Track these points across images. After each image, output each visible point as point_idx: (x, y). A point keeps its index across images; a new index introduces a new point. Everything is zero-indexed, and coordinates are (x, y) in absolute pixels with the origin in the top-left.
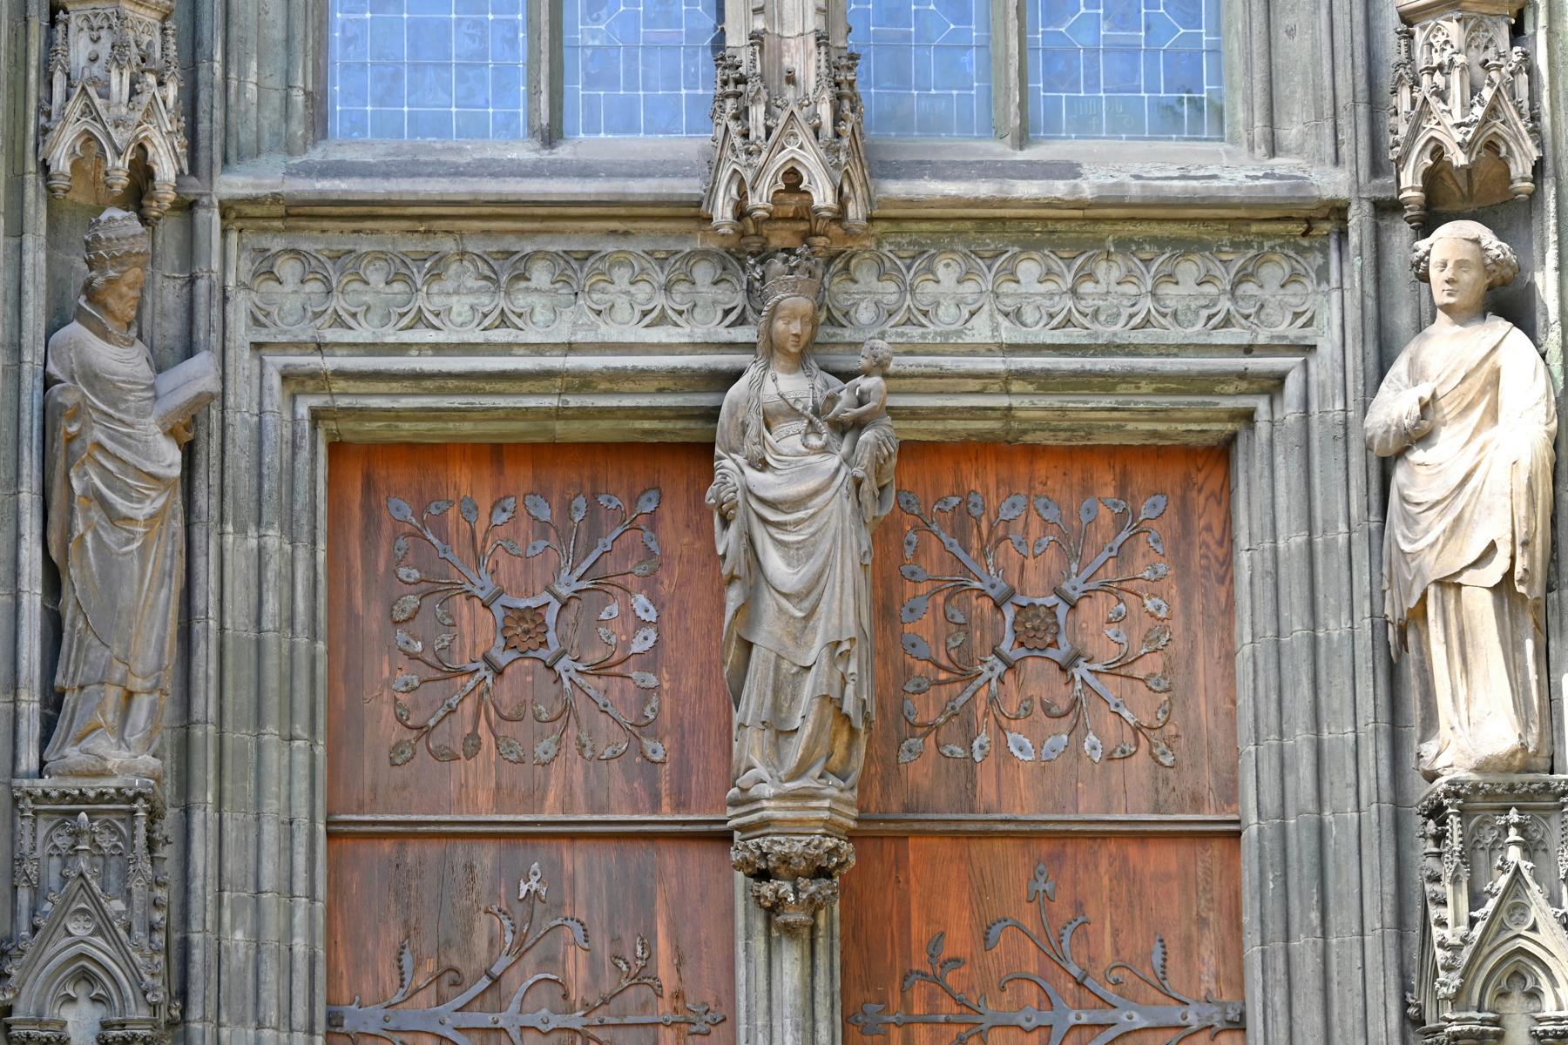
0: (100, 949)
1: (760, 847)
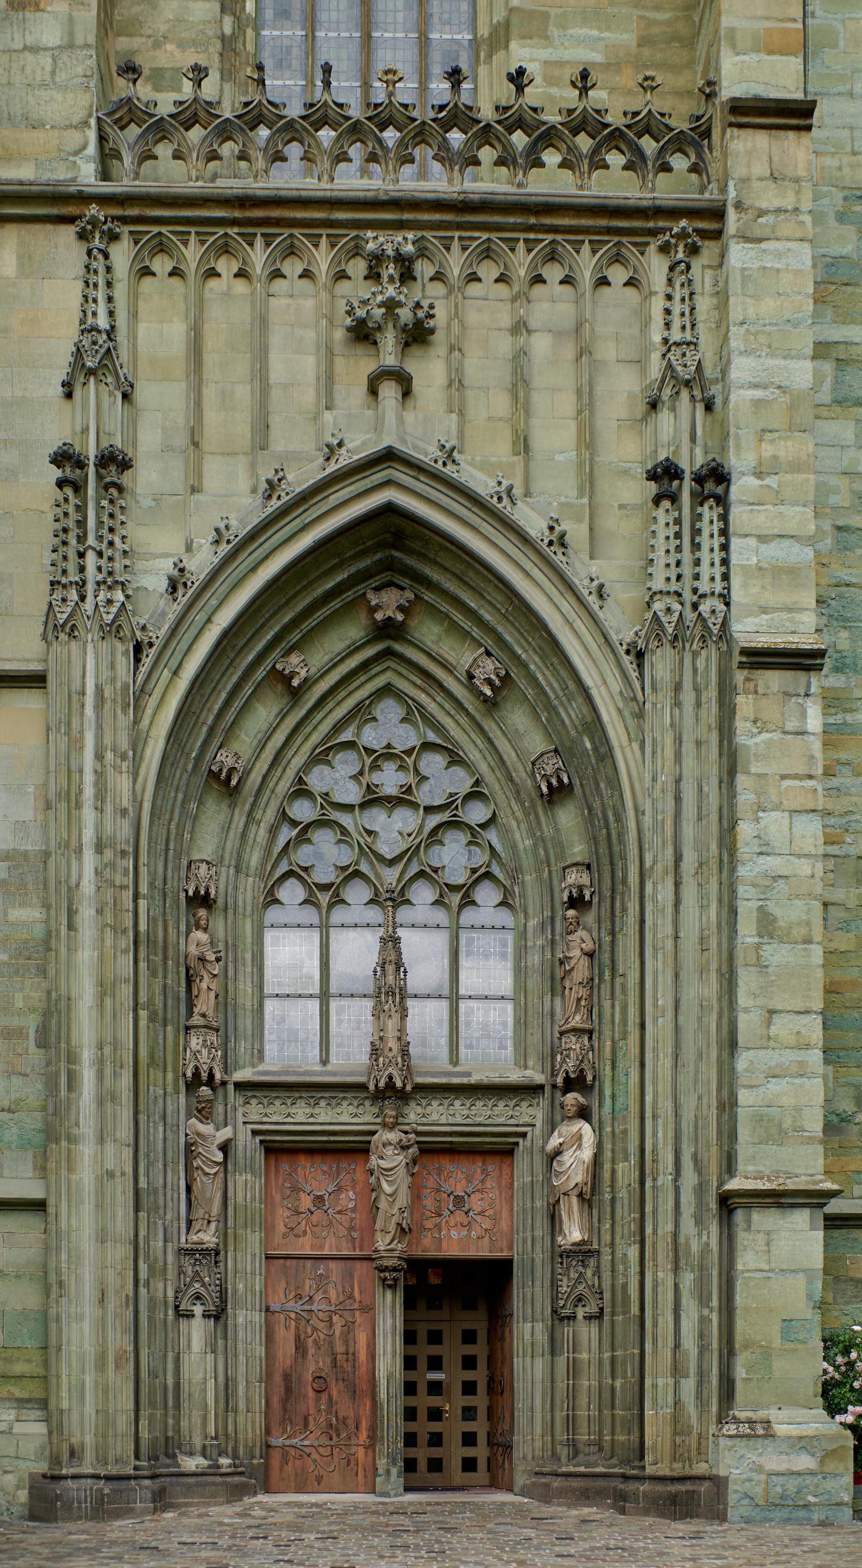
0: (202, 1291)
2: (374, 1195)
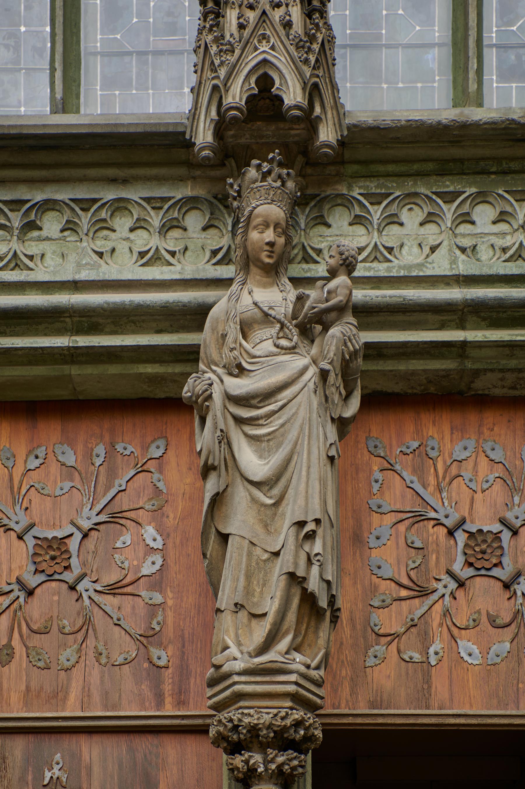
1: (231, 720)
2: (211, 486)
